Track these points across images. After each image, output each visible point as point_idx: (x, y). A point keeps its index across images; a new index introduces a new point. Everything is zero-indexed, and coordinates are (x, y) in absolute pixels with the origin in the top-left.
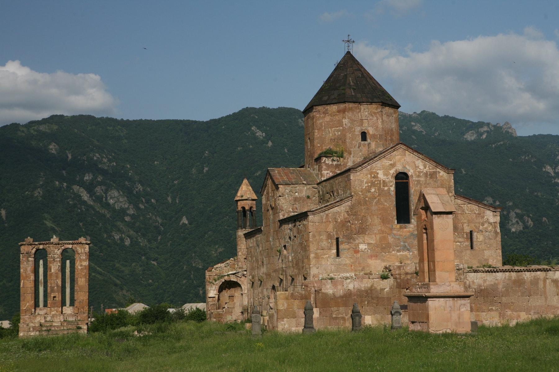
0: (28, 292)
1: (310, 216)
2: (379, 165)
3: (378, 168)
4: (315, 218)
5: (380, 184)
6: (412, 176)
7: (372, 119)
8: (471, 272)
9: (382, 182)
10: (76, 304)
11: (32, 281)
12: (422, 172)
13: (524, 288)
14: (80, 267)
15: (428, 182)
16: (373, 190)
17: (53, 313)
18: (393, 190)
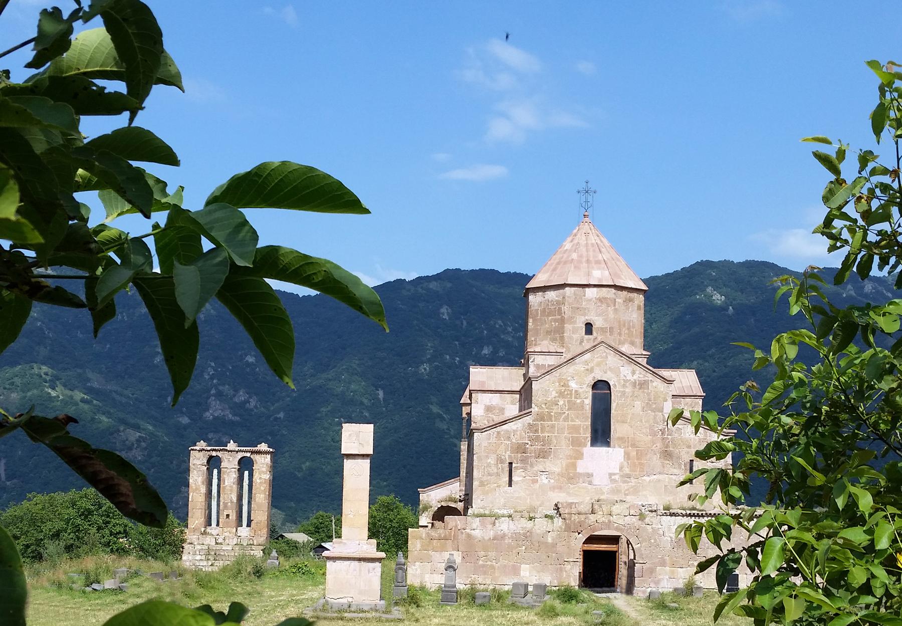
0: (198, 508)
1: (475, 434)
2: (570, 369)
5: (571, 394)
6: (615, 385)
7: (601, 306)
8: (667, 515)
9: (573, 392)
10: (253, 524)
11: (202, 495)
13: (740, 539)
14: (258, 481)
15: (635, 392)
16: (561, 403)
17: (226, 534)
18: (587, 403)
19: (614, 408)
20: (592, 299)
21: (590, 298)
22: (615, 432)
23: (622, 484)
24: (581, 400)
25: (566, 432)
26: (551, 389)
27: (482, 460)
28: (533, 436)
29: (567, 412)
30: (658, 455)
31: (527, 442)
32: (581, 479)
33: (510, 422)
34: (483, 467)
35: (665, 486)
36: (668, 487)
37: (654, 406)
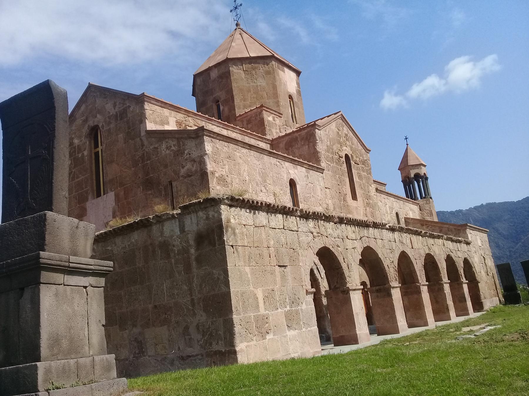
12: (113, 114)
29: (73, 171)
30: (142, 188)
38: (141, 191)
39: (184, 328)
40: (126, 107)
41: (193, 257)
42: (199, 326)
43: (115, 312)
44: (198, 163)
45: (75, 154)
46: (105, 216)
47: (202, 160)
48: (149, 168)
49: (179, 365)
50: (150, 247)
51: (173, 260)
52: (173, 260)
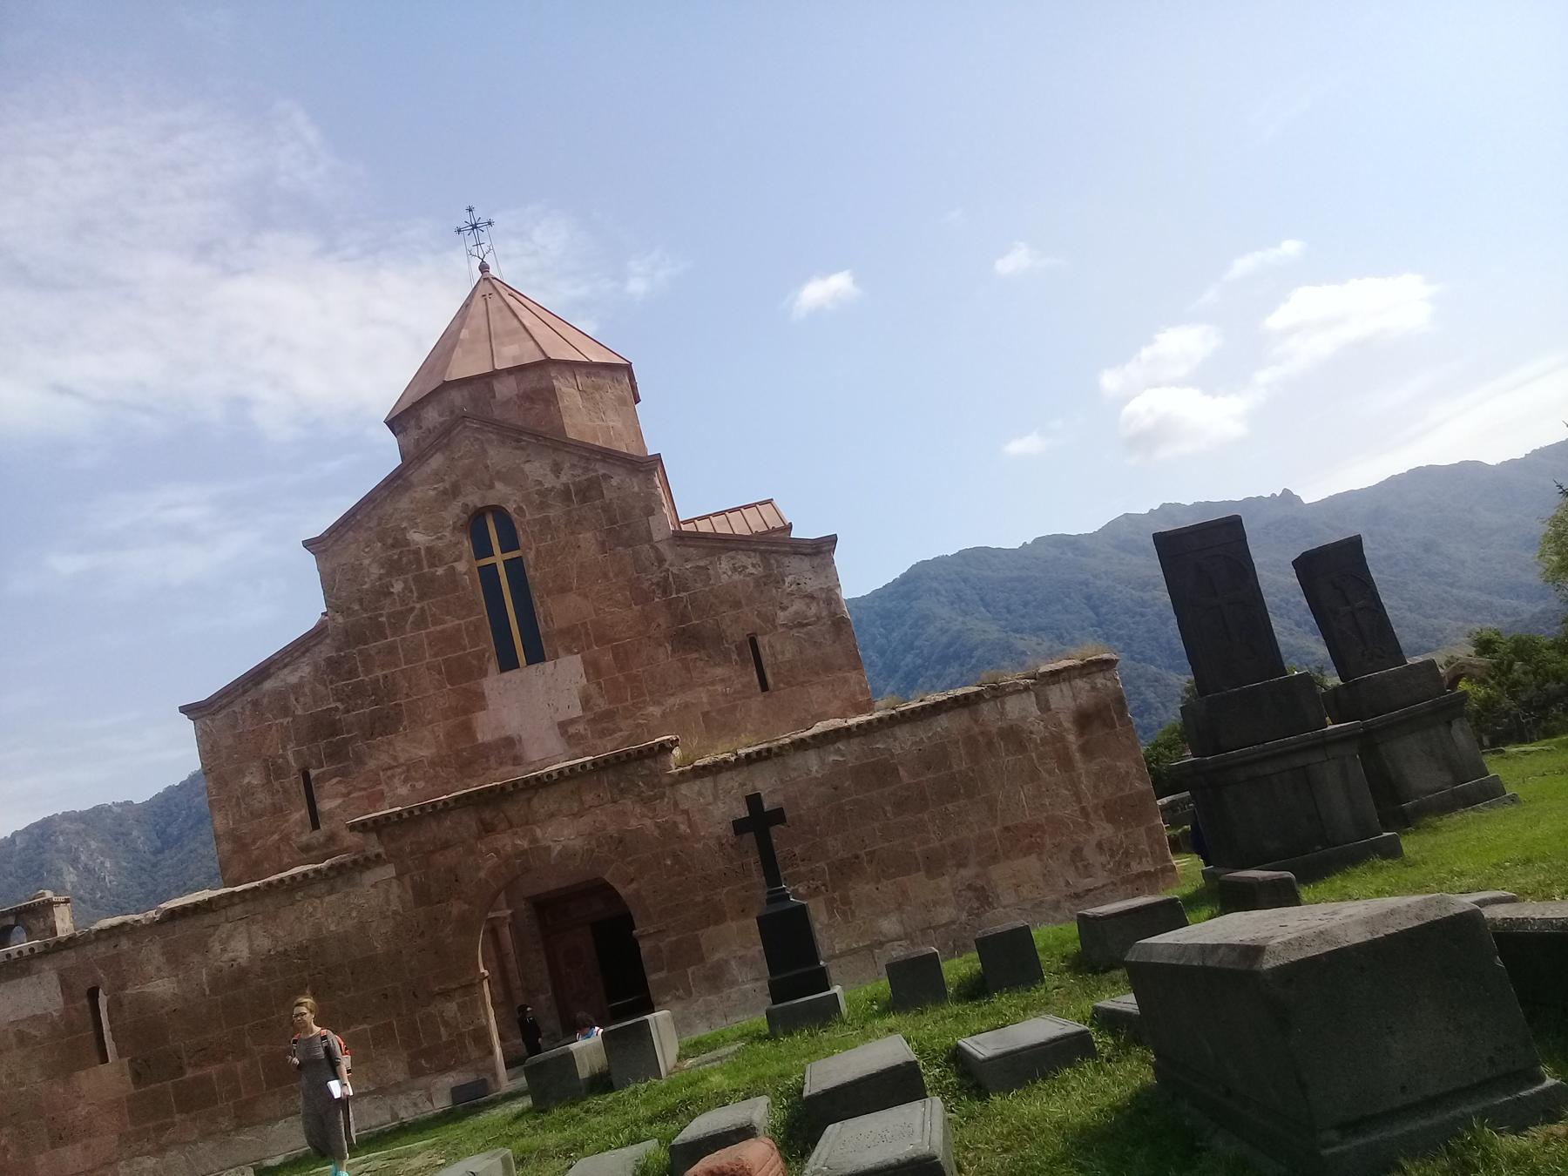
2: (404, 503)
3: (403, 514)
4: (216, 722)
5: (419, 562)
9: (423, 552)
16: (398, 587)
18: (464, 570)
19: (531, 563)
20: (511, 398)
21: (505, 399)
22: (548, 618)
23: (598, 742)
24: (446, 567)
25: (427, 655)
26: (366, 562)
27: (227, 785)
28: (348, 685)
29: (418, 606)
30: (669, 648)
31: (333, 705)
32: (492, 759)
33: (279, 669)
34: (234, 800)
35: (706, 715)
36: (714, 714)
37: (626, 533)
38: (669, 652)
39: (1073, 852)
40: (598, 477)
41: (1074, 747)
42: (1102, 845)
43: (912, 850)
44: (821, 602)
45: (420, 567)
46: (558, 710)
47: (834, 597)
48: (686, 607)
49: (1072, 907)
50: (980, 738)
51: (1033, 754)
52: (1033, 754)
